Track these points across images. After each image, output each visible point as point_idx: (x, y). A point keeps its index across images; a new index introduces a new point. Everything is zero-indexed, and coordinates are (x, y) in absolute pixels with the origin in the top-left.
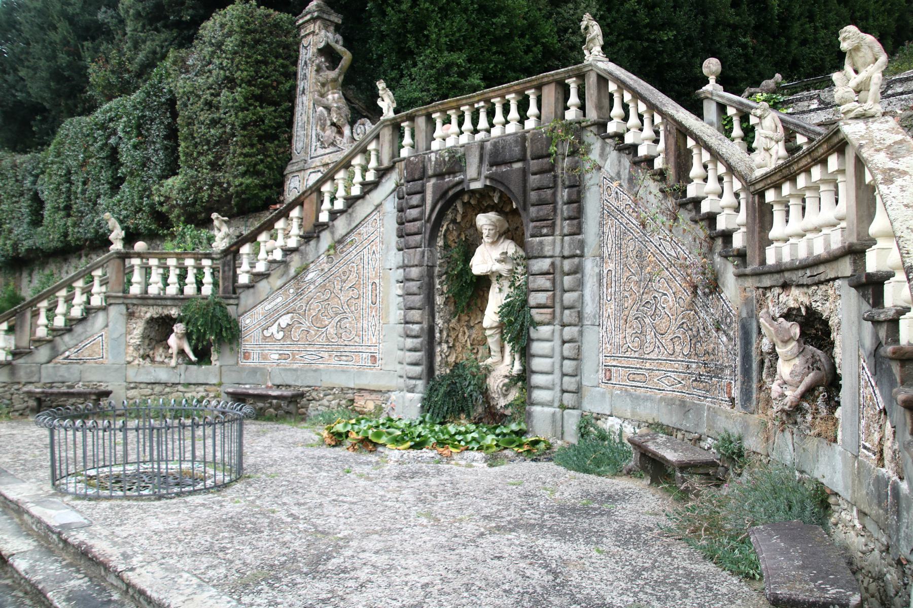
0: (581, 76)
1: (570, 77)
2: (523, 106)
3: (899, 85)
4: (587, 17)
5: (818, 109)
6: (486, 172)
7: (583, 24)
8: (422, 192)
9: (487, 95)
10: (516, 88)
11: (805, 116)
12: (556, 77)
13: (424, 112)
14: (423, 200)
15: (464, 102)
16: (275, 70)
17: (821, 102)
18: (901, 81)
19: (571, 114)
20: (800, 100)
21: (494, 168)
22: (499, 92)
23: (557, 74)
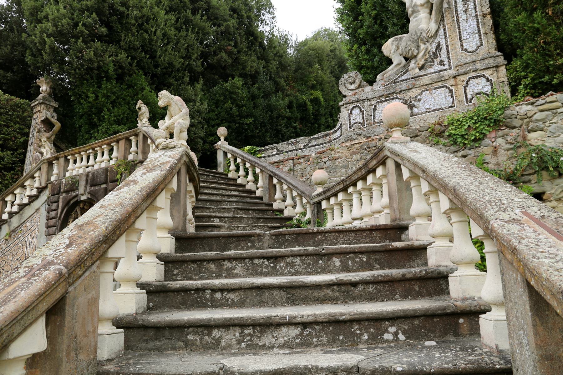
0: (137, 135)
1: (131, 136)
2: (111, 151)
3: (314, 141)
4: (140, 102)
5: (276, 154)
6: (88, 190)
7: (137, 106)
8: (58, 201)
9: (93, 146)
10: (107, 142)
11: (270, 158)
12: (125, 136)
13: (63, 155)
14: (58, 206)
15: (82, 149)
16: (14, 130)
17: (278, 150)
18: (315, 139)
19: (131, 157)
20: (267, 149)
21: (93, 188)
22: (98, 144)
23: (125, 134)
